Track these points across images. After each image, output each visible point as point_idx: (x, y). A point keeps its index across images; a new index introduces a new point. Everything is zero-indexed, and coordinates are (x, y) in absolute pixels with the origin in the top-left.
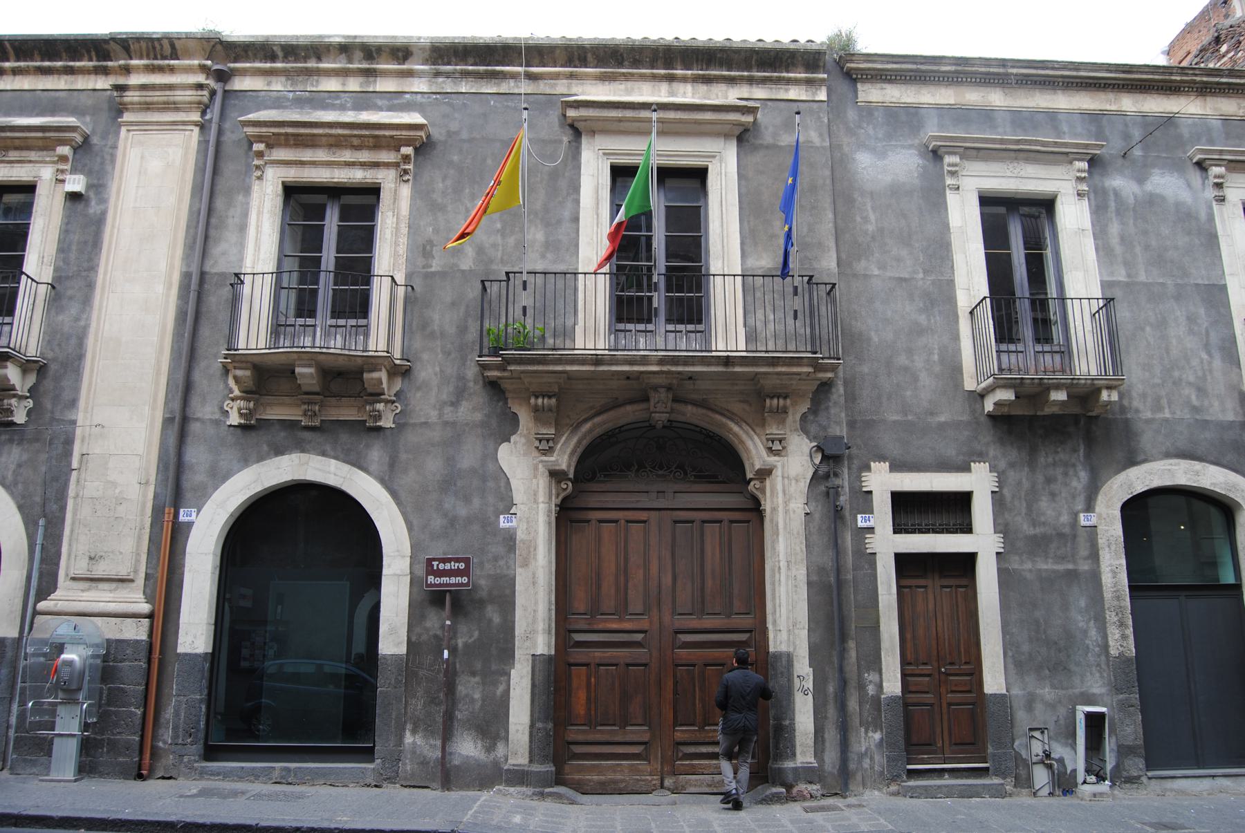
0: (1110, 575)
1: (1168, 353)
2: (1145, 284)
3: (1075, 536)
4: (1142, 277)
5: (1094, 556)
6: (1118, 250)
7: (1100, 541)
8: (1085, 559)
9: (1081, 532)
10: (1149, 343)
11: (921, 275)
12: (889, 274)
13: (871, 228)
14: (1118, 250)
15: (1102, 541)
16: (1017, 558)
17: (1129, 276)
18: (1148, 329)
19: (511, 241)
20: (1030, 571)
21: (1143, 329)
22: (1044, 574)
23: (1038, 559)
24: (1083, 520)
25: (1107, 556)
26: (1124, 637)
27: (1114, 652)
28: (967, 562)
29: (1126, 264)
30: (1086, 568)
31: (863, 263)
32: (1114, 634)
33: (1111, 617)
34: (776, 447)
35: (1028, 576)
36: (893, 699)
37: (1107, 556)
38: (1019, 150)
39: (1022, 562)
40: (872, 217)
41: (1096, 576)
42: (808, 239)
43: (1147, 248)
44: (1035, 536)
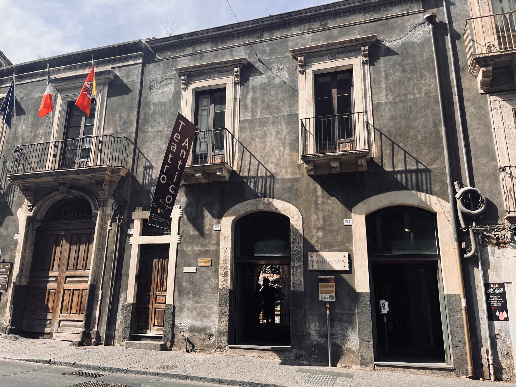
0: (224, 252)
1: (264, 149)
2: (259, 119)
3: (211, 235)
4: (259, 116)
5: (218, 244)
6: (250, 105)
7: (221, 237)
8: (214, 245)
9: (214, 233)
10: (256, 146)
11: (166, 129)
12: (154, 130)
13: (151, 112)
14: (250, 105)
15: (222, 237)
16: (186, 245)
17: (252, 116)
18: (257, 139)
19: (33, 134)
20: (191, 250)
21: (254, 140)
22: (196, 252)
23: (194, 245)
24: (215, 228)
25: (223, 244)
26: (226, 280)
27: (220, 287)
28: (166, 247)
29: (252, 111)
30: (214, 249)
31: (146, 127)
32: (221, 278)
33: (221, 271)
34: (103, 204)
35: (189, 253)
36: (129, 305)
37: (223, 244)
38: (211, 68)
39: (187, 247)
40: (152, 107)
41: (217, 252)
42: (127, 120)
43: (263, 102)
44: (195, 235)
